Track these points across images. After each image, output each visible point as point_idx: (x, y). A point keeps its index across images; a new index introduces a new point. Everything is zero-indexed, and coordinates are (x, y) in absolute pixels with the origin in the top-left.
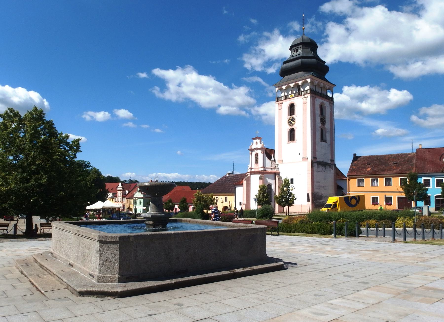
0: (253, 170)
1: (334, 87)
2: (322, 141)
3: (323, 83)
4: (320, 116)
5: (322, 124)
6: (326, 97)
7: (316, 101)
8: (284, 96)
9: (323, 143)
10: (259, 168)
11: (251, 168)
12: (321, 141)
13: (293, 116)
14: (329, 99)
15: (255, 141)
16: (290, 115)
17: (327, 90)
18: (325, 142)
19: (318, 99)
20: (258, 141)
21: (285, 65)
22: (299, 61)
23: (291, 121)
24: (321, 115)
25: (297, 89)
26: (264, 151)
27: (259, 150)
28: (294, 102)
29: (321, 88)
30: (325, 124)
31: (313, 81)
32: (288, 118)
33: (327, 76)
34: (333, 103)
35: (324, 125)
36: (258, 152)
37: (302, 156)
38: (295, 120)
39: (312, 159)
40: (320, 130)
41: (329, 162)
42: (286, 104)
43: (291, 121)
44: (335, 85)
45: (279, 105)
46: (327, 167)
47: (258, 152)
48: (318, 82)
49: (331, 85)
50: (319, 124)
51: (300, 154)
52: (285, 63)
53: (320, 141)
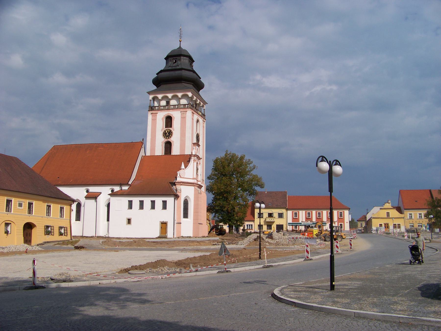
13: (170, 128)
16: (165, 128)
23: (168, 134)
33: (201, 92)
38: (172, 133)
42: (161, 116)
43: (168, 134)
45: (153, 114)
52: (161, 71)
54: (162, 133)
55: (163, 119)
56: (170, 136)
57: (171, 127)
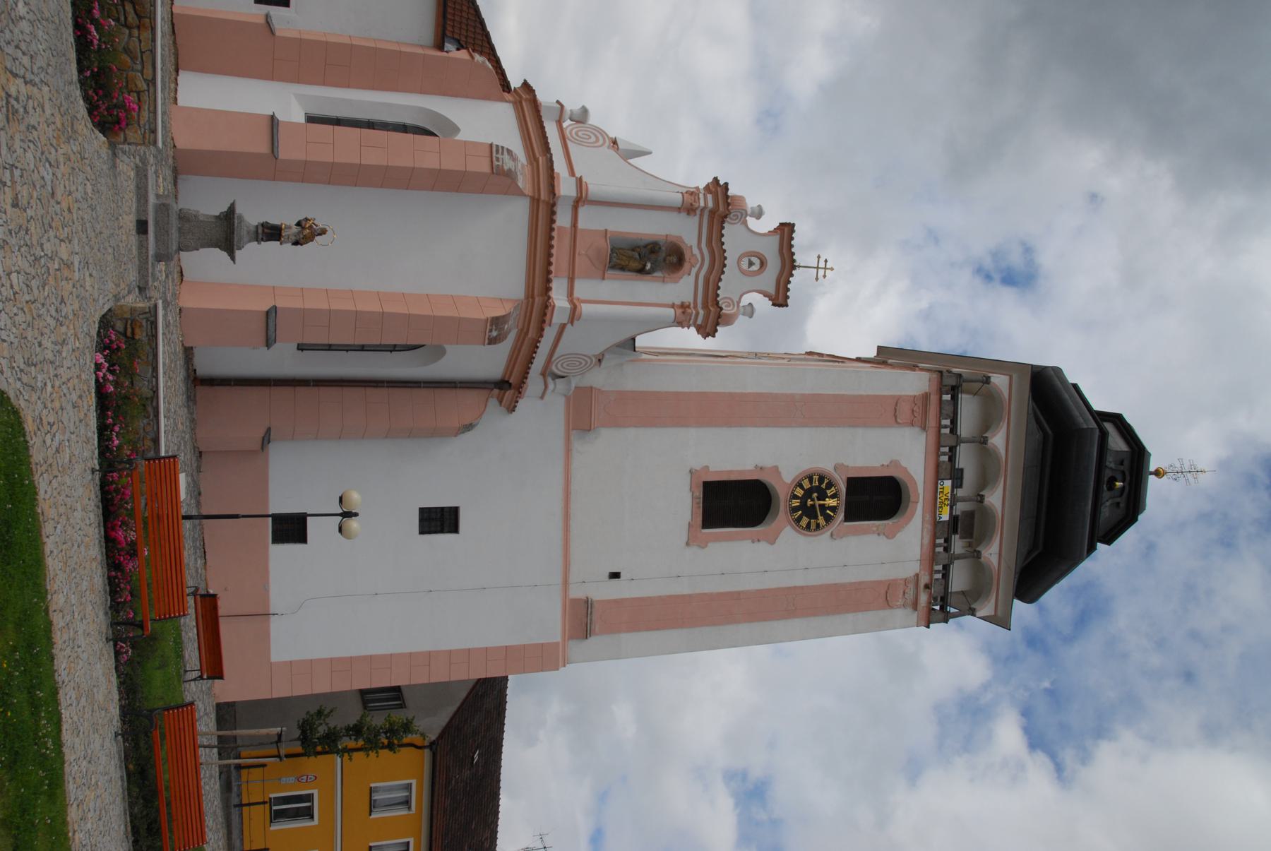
0: (563, 219)
11: (581, 200)
13: (841, 516)
15: (770, 250)
20: (769, 279)
28: (913, 514)
36: (694, 271)
47: (694, 271)
51: (615, 575)
55: (895, 463)
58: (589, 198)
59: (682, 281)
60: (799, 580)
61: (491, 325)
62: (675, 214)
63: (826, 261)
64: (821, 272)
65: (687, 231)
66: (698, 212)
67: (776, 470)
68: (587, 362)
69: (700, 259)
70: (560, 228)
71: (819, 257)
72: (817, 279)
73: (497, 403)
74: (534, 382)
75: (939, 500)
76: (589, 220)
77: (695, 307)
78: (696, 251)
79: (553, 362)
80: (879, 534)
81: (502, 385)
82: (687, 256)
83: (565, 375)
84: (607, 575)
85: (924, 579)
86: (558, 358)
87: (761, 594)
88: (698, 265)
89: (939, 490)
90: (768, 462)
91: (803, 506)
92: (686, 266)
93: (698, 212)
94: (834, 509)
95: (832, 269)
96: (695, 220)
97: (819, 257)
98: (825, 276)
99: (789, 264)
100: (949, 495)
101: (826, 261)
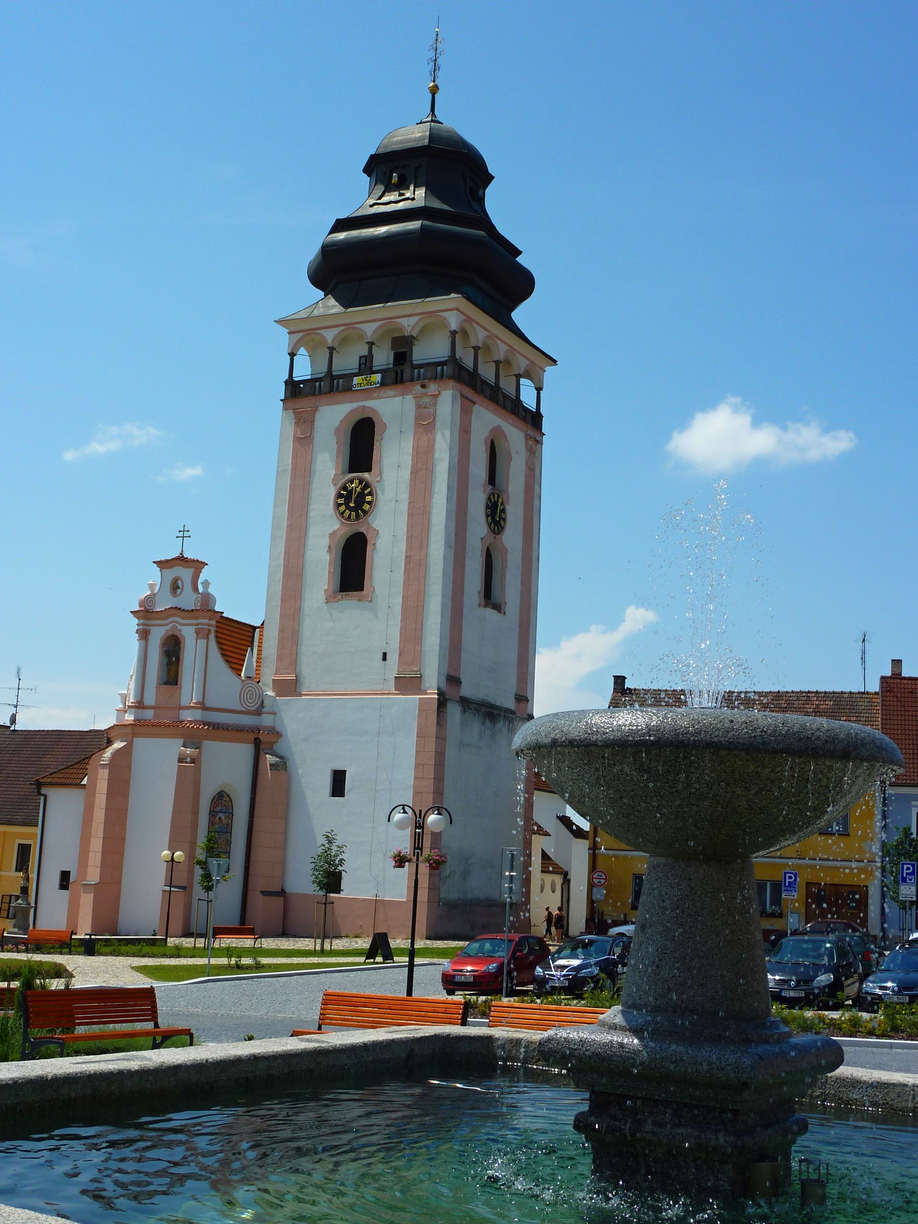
0: (149, 714)
1: (550, 370)
2: (485, 606)
3: (506, 344)
4: (484, 492)
5: (489, 525)
6: (514, 407)
7: (473, 418)
8: (329, 379)
9: (490, 613)
10: (181, 708)
11: (140, 705)
12: (483, 602)
13: (366, 475)
14: (524, 419)
16: (350, 472)
17: (518, 377)
18: (500, 612)
19: (481, 409)
20: (185, 574)
21: (341, 236)
22: (415, 225)
24: (491, 487)
25: (392, 353)
26: (213, 629)
27: (183, 618)
28: (372, 409)
29: (497, 363)
30: (503, 528)
31: (467, 327)
32: (340, 484)
34: (539, 439)
35: (499, 533)
36: (179, 627)
37: (393, 668)
39: (444, 687)
40: (482, 556)
41: (510, 704)
44: (555, 361)
46: (500, 725)
48: (487, 334)
49: (539, 360)
50: (478, 526)
51: (385, 655)
52: (341, 225)
53: (480, 605)
54: (332, 492)
55: (337, 431)
56: (366, 507)
57: (369, 469)
58: (140, 700)
59: (184, 635)
60: (404, 506)
61: (183, 762)
62: (150, 642)
63: (180, 531)
64: (186, 534)
65: (158, 634)
66: (148, 628)
67: (332, 535)
68: (249, 687)
69: (173, 624)
70: (154, 717)
71: (177, 537)
72: (189, 537)
73: (276, 744)
74: (266, 720)
75: (366, 387)
76: (150, 700)
77: (197, 625)
78: (168, 627)
79: (249, 710)
80: (382, 439)
81: (257, 743)
82: (171, 633)
83: (260, 700)
84: (384, 662)
85: (418, 388)
86: (243, 707)
87: (410, 538)
88: (177, 625)
89: (359, 388)
90: (326, 542)
91: (355, 509)
92: (176, 633)
93: (148, 628)
94: (361, 482)
95: (184, 526)
96: (153, 629)
97: (177, 537)
98: (188, 531)
99: (182, 560)
100: (363, 377)
101: (180, 531)
